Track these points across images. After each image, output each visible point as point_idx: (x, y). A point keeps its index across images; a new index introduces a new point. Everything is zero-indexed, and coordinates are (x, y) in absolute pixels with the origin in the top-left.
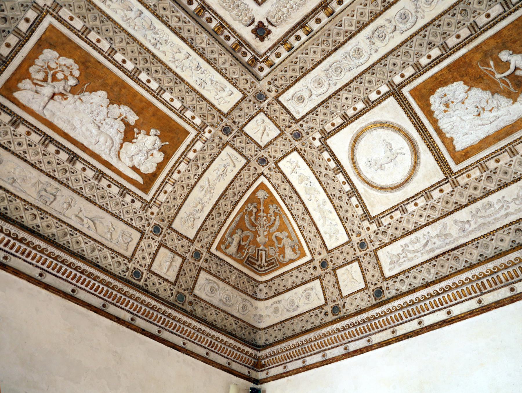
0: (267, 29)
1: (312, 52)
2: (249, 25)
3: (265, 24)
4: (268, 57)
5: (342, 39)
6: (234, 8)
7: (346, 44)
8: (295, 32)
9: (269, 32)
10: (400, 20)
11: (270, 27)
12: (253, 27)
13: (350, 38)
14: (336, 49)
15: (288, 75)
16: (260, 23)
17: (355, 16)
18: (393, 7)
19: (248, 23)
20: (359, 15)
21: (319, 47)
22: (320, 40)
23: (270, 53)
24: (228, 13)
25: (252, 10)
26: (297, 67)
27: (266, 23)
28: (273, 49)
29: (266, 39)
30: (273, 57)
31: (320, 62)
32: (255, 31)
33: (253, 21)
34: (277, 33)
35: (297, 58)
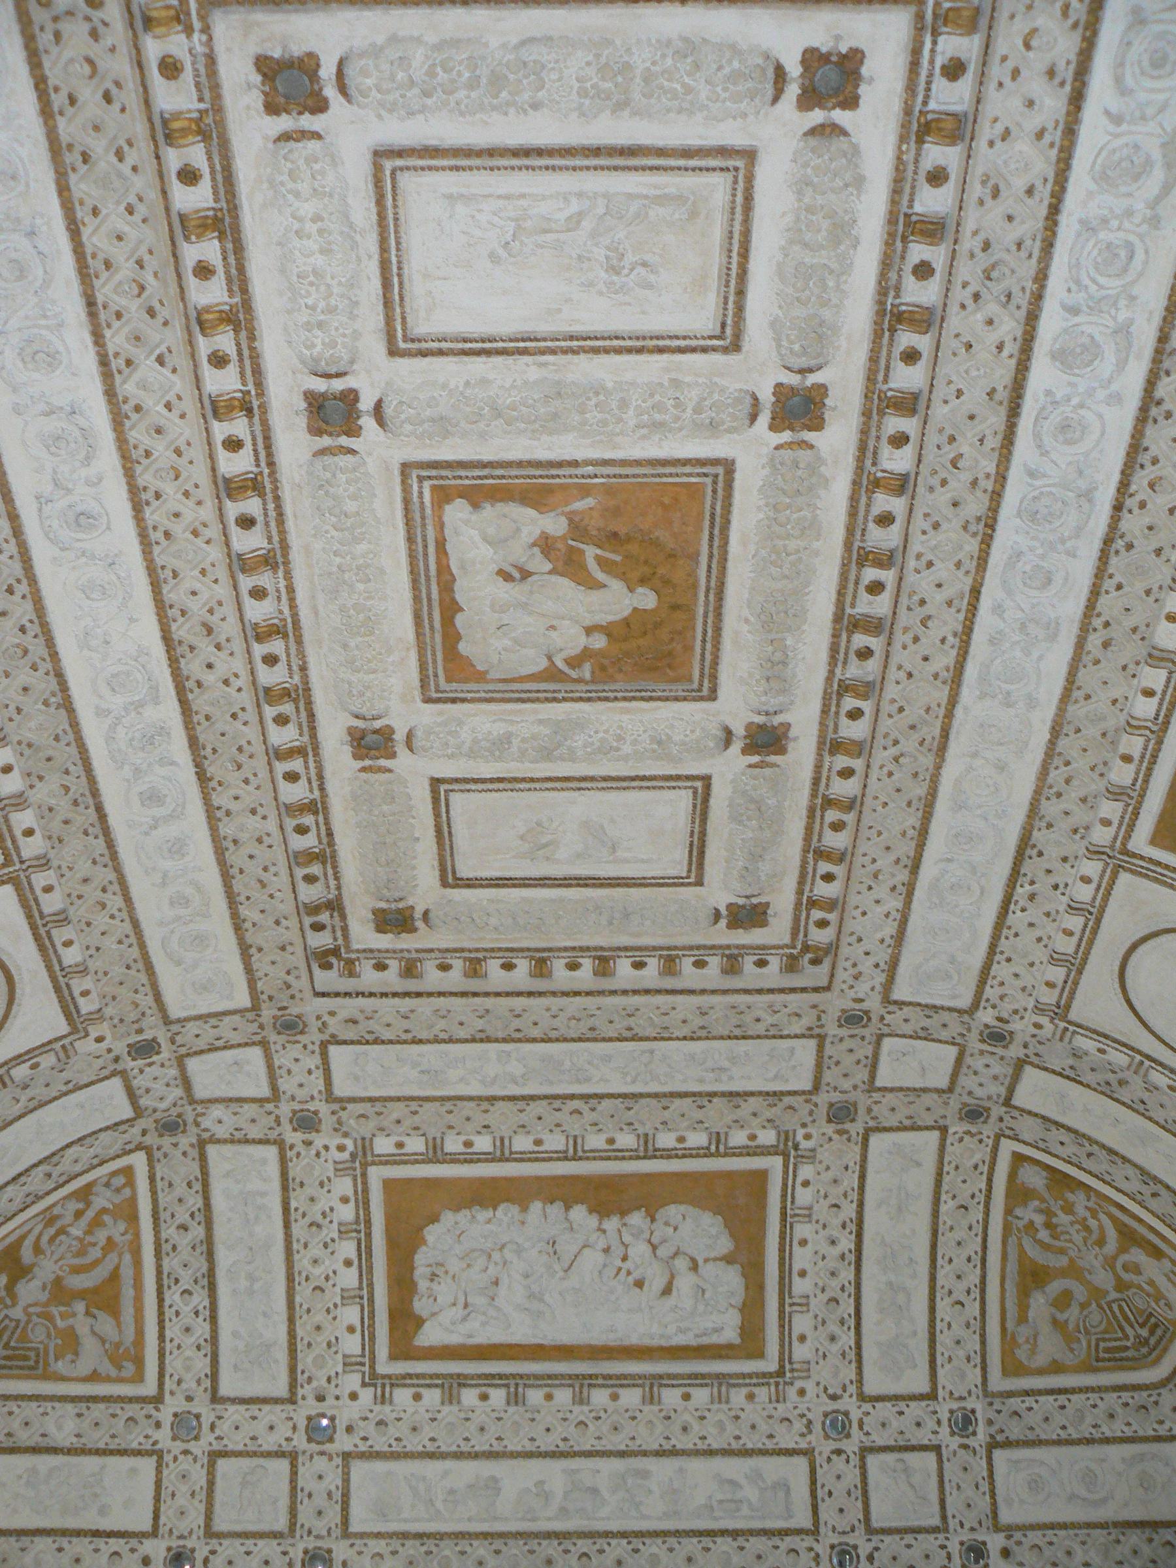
0: (288, 112)
1: (127, 229)
2: (341, 64)
3: (307, 115)
4: (189, 30)
5: (116, 340)
6: (431, 73)
7: (89, 340)
8: (213, 179)
9: (272, 109)
10: (79, 509)
11: (285, 123)
12: (327, 71)
13: (104, 362)
14: (91, 303)
15: (89, 95)
16: (320, 106)
17: (165, 411)
18: (128, 506)
19: (350, 71)
20: (162, 422)
21: (131, 264)
22: (150, 279)
23: (200, 49)
24: (431, 38)
25: (380, 117)
26: (98, 146)
27: (307, 121)
28: (202, 71)
29: (257, 79)
30: (177, 44)
31: (74, 230)
32: (307, 65)
33: (343, 89)
34: (251, 128)
35: (135, 169)
